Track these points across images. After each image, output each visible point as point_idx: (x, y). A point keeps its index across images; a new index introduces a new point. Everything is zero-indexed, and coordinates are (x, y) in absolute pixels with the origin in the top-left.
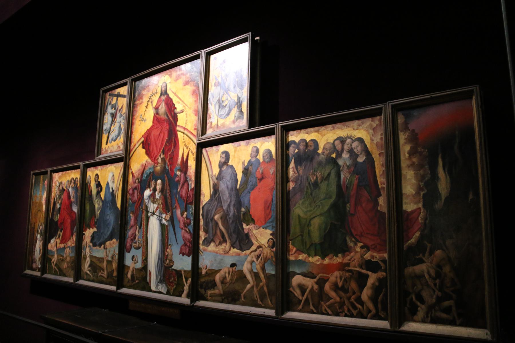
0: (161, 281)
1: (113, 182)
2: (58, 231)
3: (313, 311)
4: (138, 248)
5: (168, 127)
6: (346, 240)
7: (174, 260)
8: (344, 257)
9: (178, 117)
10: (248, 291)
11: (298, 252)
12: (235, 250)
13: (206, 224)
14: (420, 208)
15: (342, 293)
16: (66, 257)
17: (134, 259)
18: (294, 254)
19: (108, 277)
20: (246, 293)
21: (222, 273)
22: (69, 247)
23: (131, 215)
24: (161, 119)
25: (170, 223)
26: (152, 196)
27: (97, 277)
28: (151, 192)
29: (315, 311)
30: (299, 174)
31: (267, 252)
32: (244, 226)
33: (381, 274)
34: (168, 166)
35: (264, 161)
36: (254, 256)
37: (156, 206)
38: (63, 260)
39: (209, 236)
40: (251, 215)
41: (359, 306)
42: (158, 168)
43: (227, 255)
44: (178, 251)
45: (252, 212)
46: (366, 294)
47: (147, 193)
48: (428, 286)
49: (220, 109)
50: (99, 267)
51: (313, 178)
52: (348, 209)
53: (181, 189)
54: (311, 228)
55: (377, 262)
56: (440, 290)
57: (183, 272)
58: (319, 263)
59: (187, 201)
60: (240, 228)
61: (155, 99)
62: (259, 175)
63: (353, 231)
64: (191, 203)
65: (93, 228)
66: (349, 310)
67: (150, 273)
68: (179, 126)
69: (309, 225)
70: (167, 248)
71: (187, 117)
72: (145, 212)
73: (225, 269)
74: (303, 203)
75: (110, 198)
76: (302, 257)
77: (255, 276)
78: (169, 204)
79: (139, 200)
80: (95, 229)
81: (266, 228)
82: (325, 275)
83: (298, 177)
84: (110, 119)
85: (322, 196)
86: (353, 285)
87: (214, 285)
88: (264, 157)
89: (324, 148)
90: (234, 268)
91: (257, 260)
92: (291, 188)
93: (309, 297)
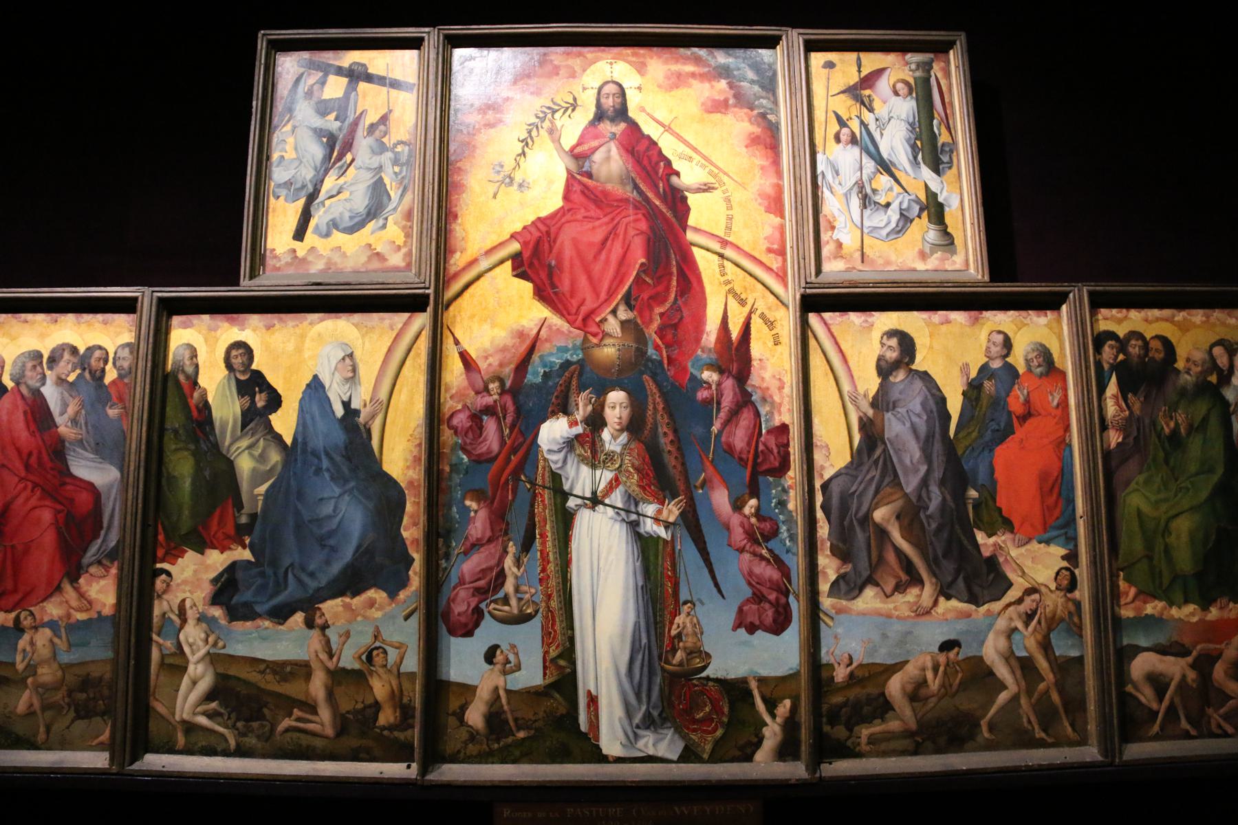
0: (649, 723)
1: (353, 377)
3: (1187, 732)
4: (522, 619)
5: (643, 225)
7: (707, 648)
9: (690, 202)
10: (1003, 708)
11: (1141, 597)
12: (954, 603)
17: (499, 658)
18: (1133, 601)
20: (997, 713)
21: (911, 670)
22: (53, 625)
23: (473, 505)
24: (605, 193)
25: (682, 532)
26: (586, 443)
28: (579, 429)
30: (1131, 413)
31: (1054, 602)
32: (980, 537)
34: (657, 347)
35: (1029, 370)
36: (1015, 616)
37: (606, 476)
39: (855, 568)
40: (1000, 510)
42: (609, 352)
43: (927, 618)
44: (730, 617)
45: (1002, 501)
49: (867, 212)
51: (1168, 425)
53: (727, 422)
54: (1172, 540)
57: (753, 685)
58: (1195, 619)
59: (755, 464)
60: (966, 542)
61: (572, 128)
67: (593, 700)
68: (696, 230)
69: (1166, 531)
70: (676, 613)
71: (730, 208)
74: (1147, 482)
76: (1154, 608)
77: (1023, 668)
79: (514, 450)
80: (247, 555)
81: (1048, 542)
82: (1211, 646)
83: (1129, 420)
84: (316, 151)
85: (1193, 468)
87: (883, 707)
88: (1027, 361)
89: (1188, 360)
90: (952, 654)
91: (1027, 625)
92: (1113, 445)
93: (1177, 701)
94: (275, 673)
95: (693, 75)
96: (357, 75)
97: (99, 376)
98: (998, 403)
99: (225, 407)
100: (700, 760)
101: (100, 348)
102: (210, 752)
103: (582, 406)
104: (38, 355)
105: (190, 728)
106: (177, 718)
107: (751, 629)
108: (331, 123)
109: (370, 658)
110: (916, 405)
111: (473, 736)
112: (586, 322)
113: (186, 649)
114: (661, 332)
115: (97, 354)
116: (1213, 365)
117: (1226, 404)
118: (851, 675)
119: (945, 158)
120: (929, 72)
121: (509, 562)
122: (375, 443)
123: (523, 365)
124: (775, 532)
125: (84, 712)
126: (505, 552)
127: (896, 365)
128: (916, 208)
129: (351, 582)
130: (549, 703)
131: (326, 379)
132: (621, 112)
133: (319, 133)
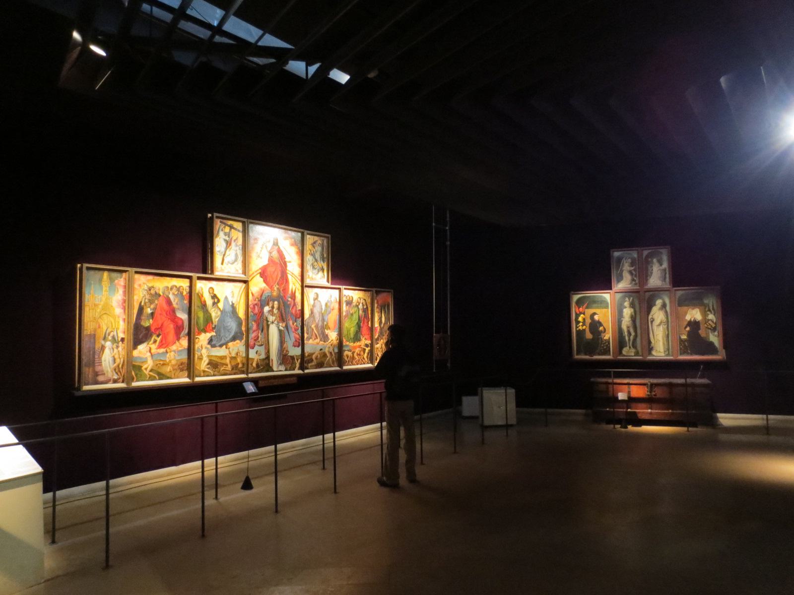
0: (281, 364)
4: (262, 345)
5: (280, 269)
13: (308, 330)
19: (233, 369)
21: (316, 354)
22: (174, 351)
23: (253, 323)
26: (271, 312)
27: (219, 372)
28: (270, 309)
32: (326, 330)
37: (274, 318)
38: (163, 364)
42: (275, 294)
44: (292, 345)
45: (329, 324)
62: (332, 308)
64: (299, 318)
65: (210, 333)
67: (272, 360)
72: (265, 322)
73: (317, 352)
80: (214, 334)
84: (224, 244)
86: (362, 353)
87: (312, 361)
94: (220, 358)
96: (231, 227)
97: (182, 293)
101: (181, 286)
102: (208, 376)
103: (271, 305)
104: (167, 287)
105: (204, 371)
106: (202, 369)
107: (295, 346)
108: (227, 238)
109: (237, 354)
111: (254, 368)
112: (271, 288)
113: (203, 355)
114: (283, 290)
115: (181, 288)
117: (359, 308)
121: (259, 334)
122: (237, 310)
123: (261, 296)
125: (182, 370)
126: (259, 332)
129: (234, 339)
130: (265, 361)
133: (225, 240)
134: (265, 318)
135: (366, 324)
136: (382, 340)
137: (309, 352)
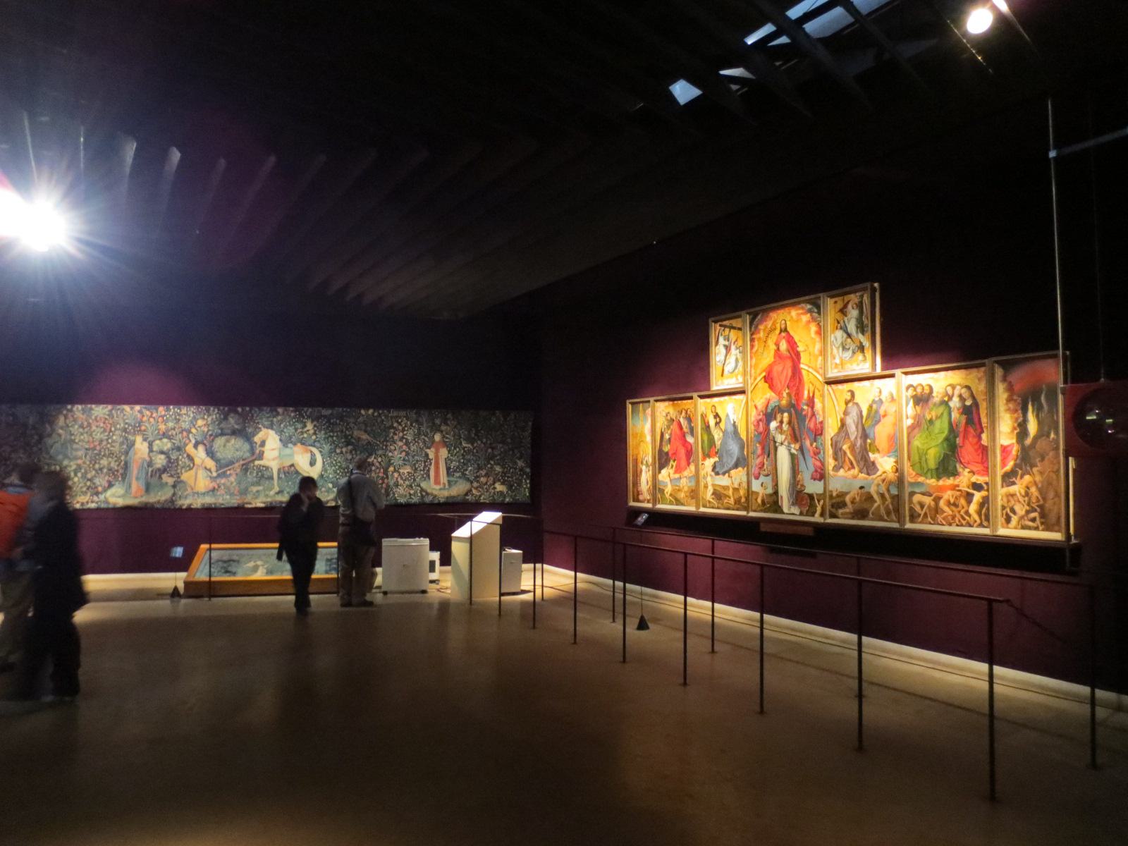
0: (793, 504)
2: (670, 461)
4: (767, 475)
6: (955, 467)
7: (805, 484)
8: (955, 479)
12: (863, 475)
14: (1013, 444)
15: (954, 508)
16: (683, 487)
19: (735, 503)
22: (686, 477)
23: (758, 445)
25: (800, 452)
26: (780, 428)
27: (722, 504)
28: (778, 424)
29: (932, 522)
32: (870, 454)
33: (984, 493)
35: (886, 400)
37: (784, 437)
38: (679, 490)
41: (967, 518)
42: (784, 402)
44: (810, 476)
46: (973, 508)
47: (773, 425)
48: (1019, 502)
50: (724, 494)
52: (957, 442)
55: (980, 484)
56: (1029, 505)
58: (934, 484)
63: (961, 459)
66: (959, 521)
67: (782, 497)
69: (926, 454)
72: (772, 443)
74: (921, 436)
75: (730, 429)
78: (798, 436)
80: (717, 459)
81: (889, 457)
84: (723, 351)
85: (937, 431)
86: (963, 502)
87: (844, 505)
93: (927, 511)
95: (802, 314)
98: (877, 412)
99: (712, 422)
100: (804, 515)
102: (713, 508)
107: (815, 479)
110: (855, 414)
111: (759, 505)
112: (779, 394)
116: (947, 394)
117: (950, 408)
118: (837, 495)
119: (866, 329)
120: (862, 298)
121: (765, 460)
124: (820, 453)
127: (850, 401)
128: (857, 349)
129: (736, 466)
131: (729, 414)
132: (786, 330)
134: (771, 438)
135: (972, 440)
136: (1027, 478)
137: (840, 490)
